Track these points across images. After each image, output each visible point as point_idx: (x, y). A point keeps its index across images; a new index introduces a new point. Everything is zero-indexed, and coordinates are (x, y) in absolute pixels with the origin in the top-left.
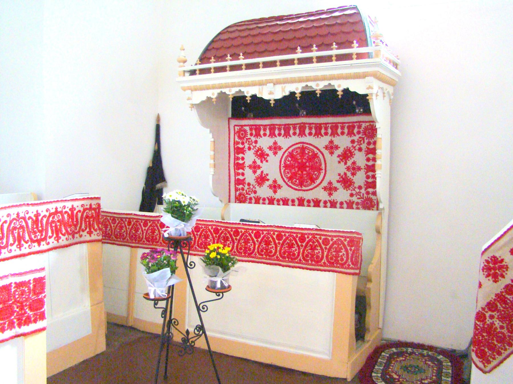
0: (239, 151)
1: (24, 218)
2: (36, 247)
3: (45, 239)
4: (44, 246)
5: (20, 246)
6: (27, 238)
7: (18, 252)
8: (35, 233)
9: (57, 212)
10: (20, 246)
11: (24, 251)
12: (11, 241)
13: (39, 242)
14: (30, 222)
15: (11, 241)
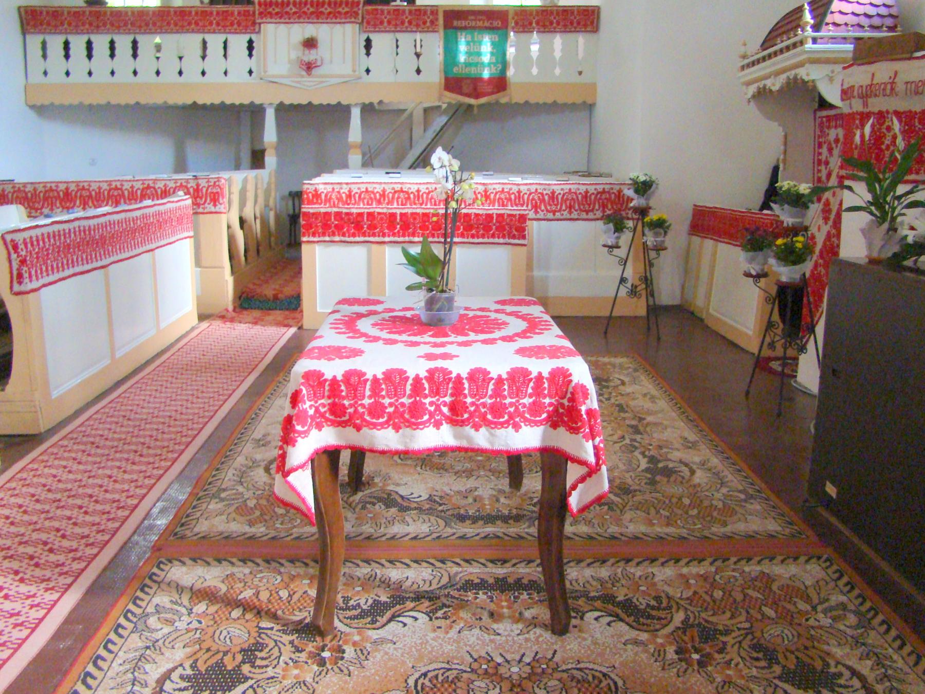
0: (820, 145)
1: (575, 193)
2: (584, 215)
3: (592, 210)
4: (591, 215)
5: (570, 213)
6: (577, 207)
7: (568, 216)
8: (584, 205)
9: (604, 192)
10: (570, 213)
11: (573, 216)
12: (564, 207)
13: (587, 212)
14: (580, 196)
15: (564, 207)
